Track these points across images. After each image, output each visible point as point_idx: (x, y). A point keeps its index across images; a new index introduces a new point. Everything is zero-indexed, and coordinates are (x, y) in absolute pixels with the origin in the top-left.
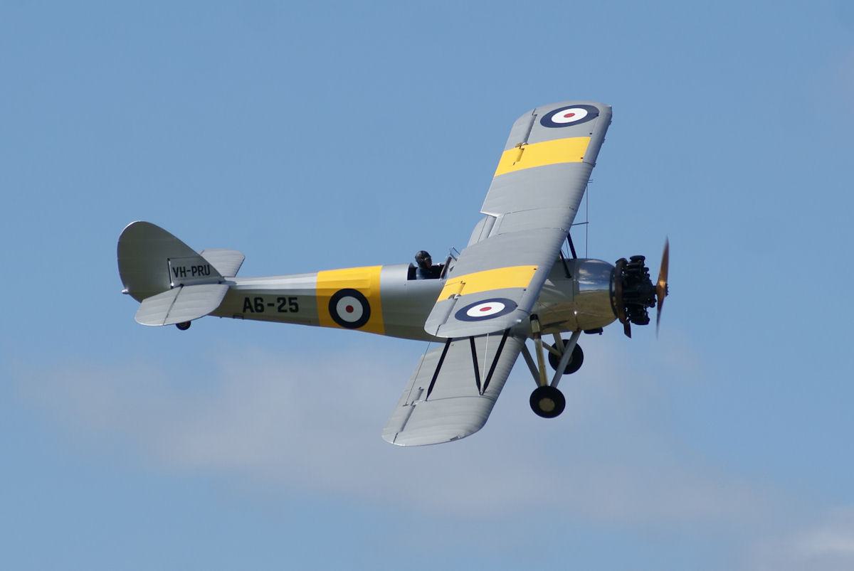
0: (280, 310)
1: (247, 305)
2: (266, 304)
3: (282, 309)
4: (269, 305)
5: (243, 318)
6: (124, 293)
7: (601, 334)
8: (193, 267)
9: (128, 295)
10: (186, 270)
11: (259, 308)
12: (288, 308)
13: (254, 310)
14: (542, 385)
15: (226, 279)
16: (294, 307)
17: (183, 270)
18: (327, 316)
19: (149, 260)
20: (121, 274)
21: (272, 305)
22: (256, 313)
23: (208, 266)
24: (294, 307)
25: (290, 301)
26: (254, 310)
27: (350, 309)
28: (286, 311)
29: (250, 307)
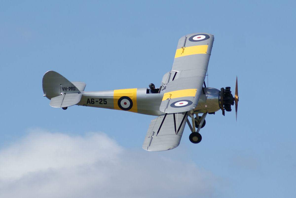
0: (100, 103)
1: (88, 101)
3: (101, 103)
4: (96, 101)
5: (86, 106)
6: (44, 96)
7: (214, 114)
8: (69, 88)
9: (46, 97)
10: (67, 88)
11: (93, 102)
12: (103, 102)
14: (194, 132)
15: (81, 92)
16: (105, 102)
17: (66, 88)
18: (118, 106)
19: (53, 85)
20: (43, 89)
21: (98, 101)
22: (91, 104)
23: (75, 87)
24: (105, 102)
27: (125, 103)
28: (102, 104)
29: (89, 102)
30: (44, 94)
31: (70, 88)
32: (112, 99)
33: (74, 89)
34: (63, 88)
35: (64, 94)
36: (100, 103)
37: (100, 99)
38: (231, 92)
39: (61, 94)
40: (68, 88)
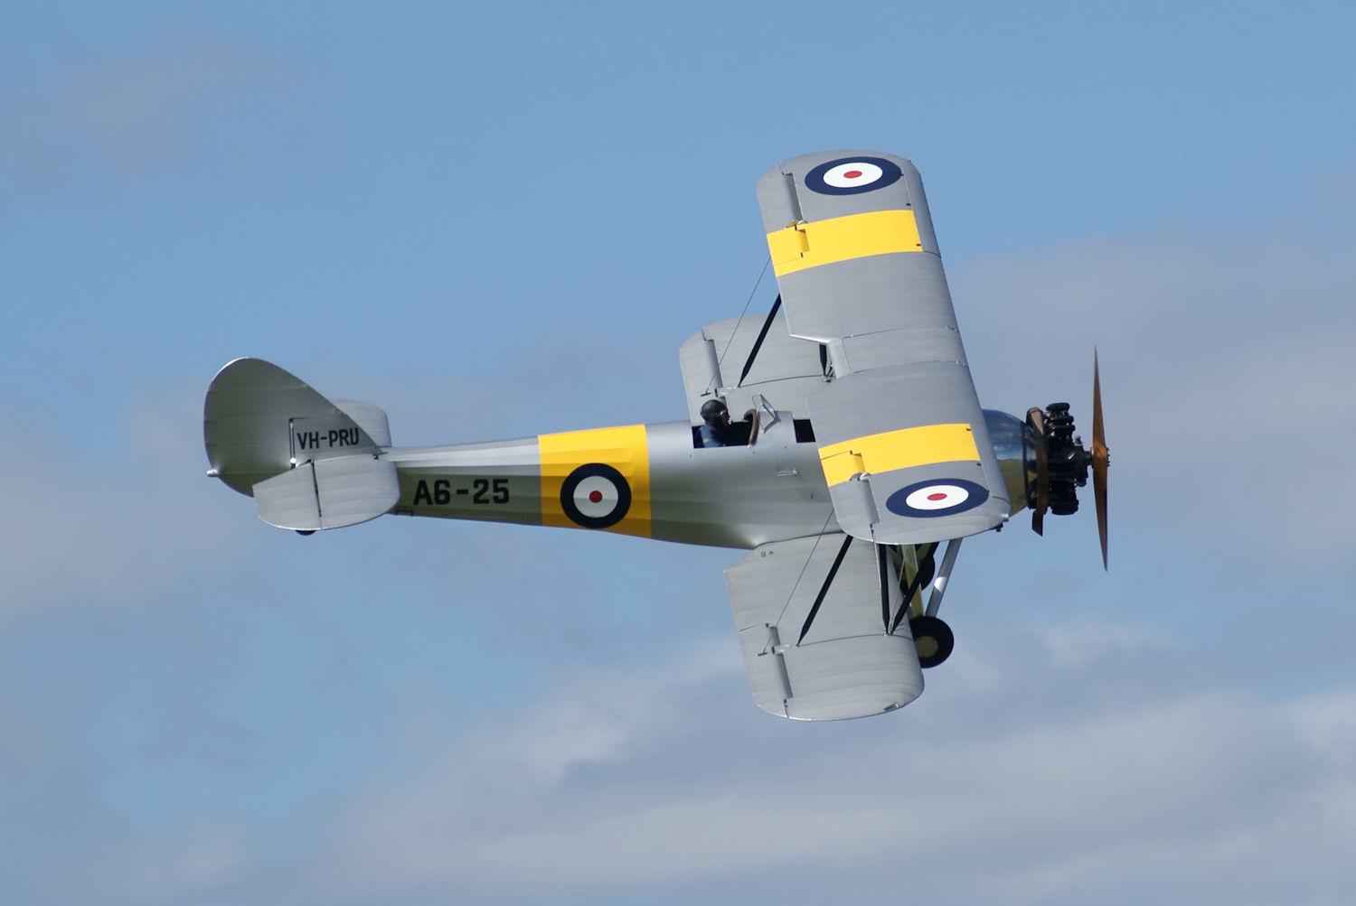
0: (477, 499)
1: (422, 492)
2: (455, 492)
3: (481, 498)
5: (412, 513)
8: (331, 433)
9: (217, 478)
10: (320, 436)
11: (442, 497)
15: (384, 450)
16: (501, 495)
17: (314, 437)
18: (560, 510)
19: (252, 422)
23: (356, 430)
24: (501, 495)
27: (596, 497)
28: (487, 501)
29: (427, 495)
31: (334, 436)
32: (532, 480)
33: (354, 441)
34: (302, 438)
35: (309, 465)
36: (477, 499)
37: (476, 483)
39: (293, 466)
40: (327, 435)
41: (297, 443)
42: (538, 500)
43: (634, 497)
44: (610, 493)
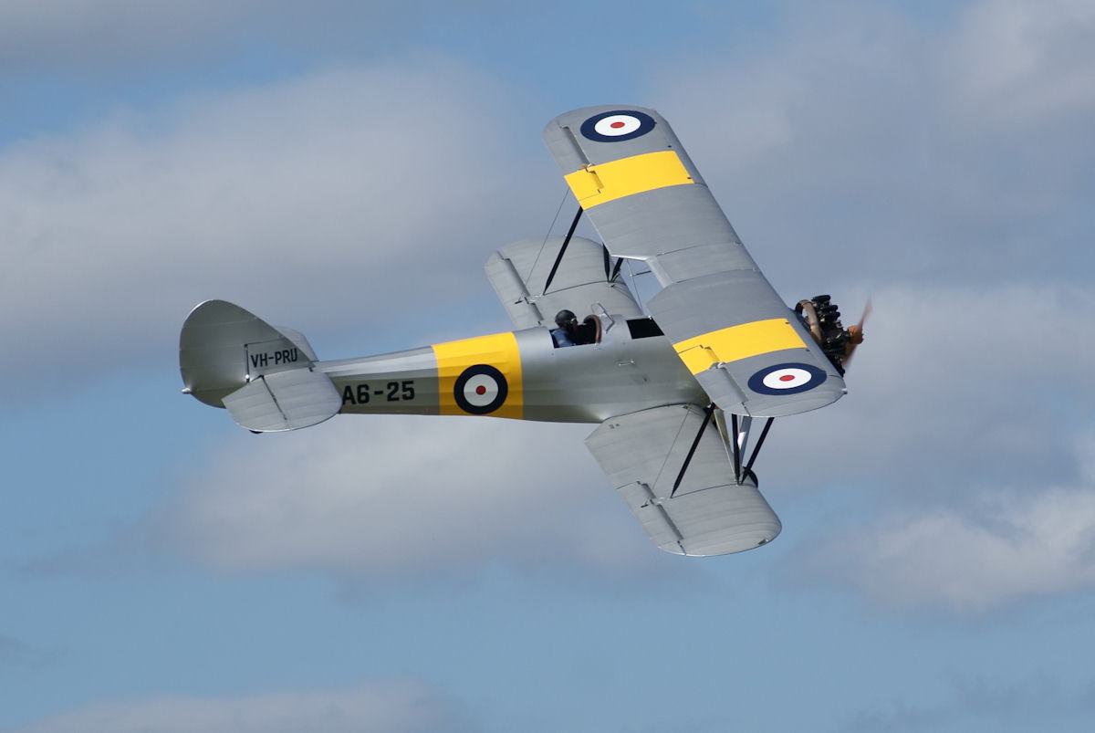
0: (390, 398)
1: (348, 395)
6: (185, 393)
8: (276, 353)
9: (190, 396)
11: (363, 398)
13: (356, 400)
17: (263, 358)
25: (404, 386)
26: (356, 400)
27: (481, 390)
28: (397, 399)
29: (352, 398)
30: (186, 387)
31: (278, 356)
32: (432, 380)
35: (260, 379)
36: (390, 398)
37: (389, 386)
38: (839, 314)
39: (248, 380)
40: (273, 355)
41: (250, 357)
42: (436, 396)
43: (510, 389)
44: (492, 386)
